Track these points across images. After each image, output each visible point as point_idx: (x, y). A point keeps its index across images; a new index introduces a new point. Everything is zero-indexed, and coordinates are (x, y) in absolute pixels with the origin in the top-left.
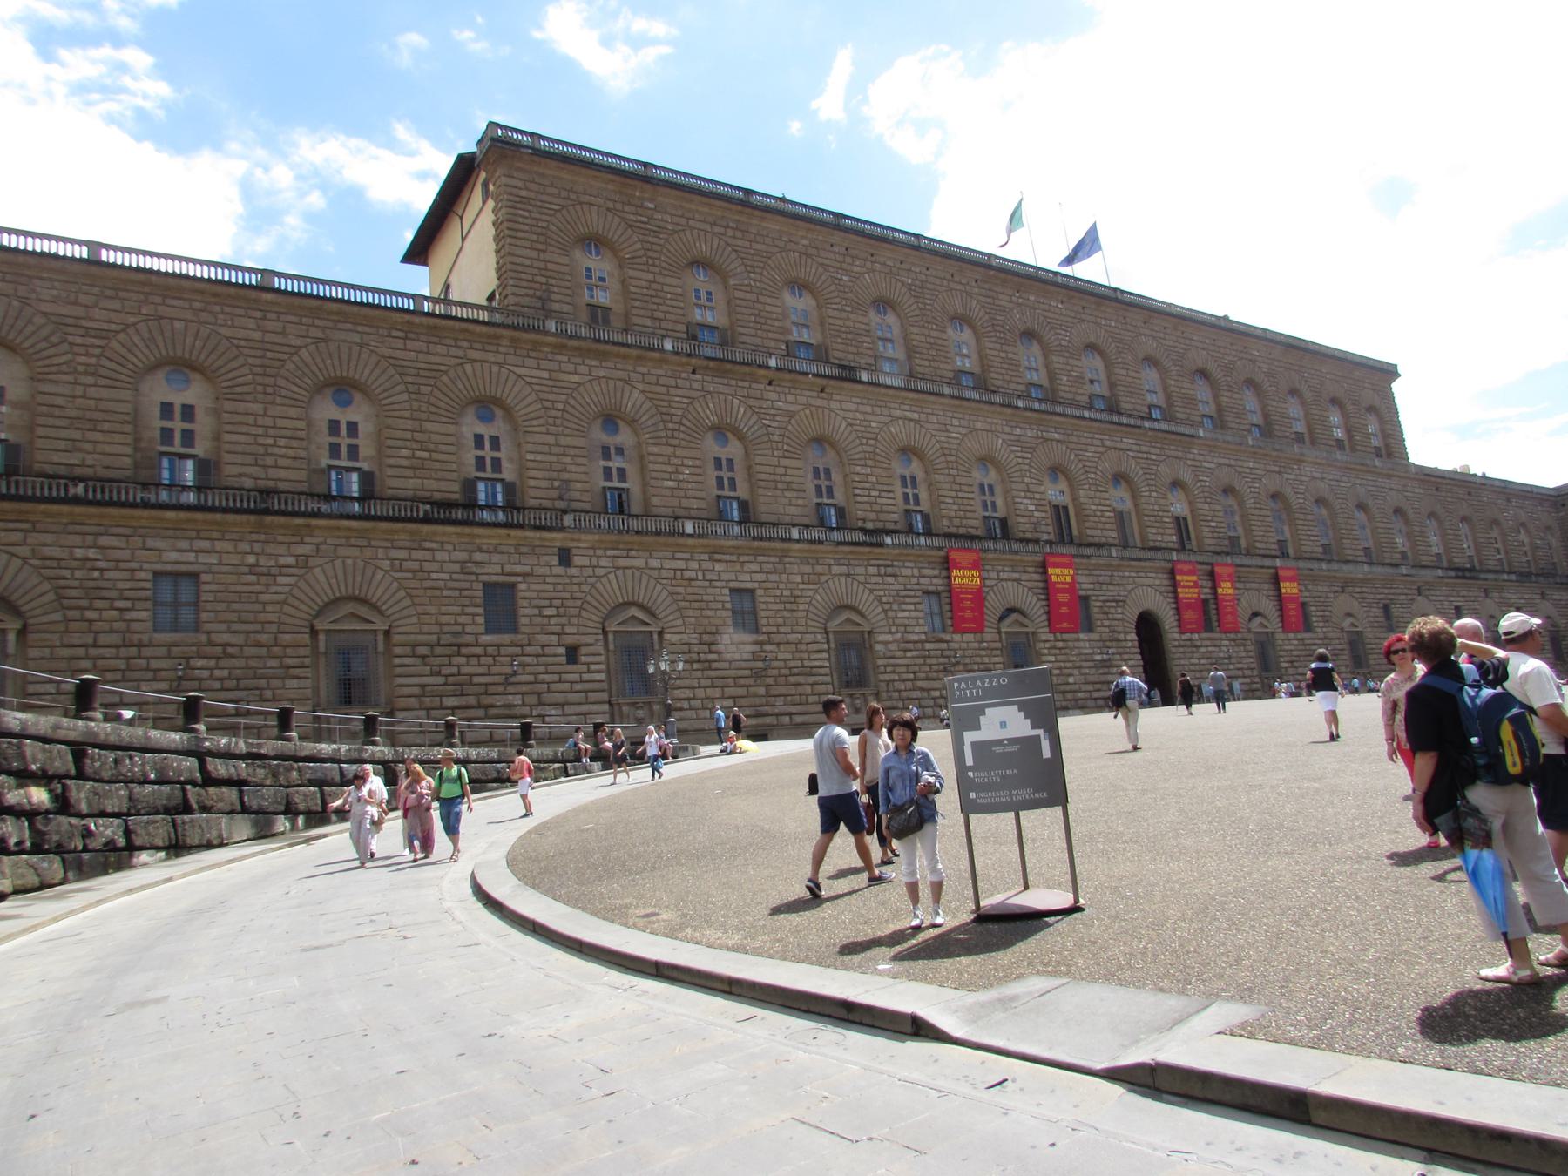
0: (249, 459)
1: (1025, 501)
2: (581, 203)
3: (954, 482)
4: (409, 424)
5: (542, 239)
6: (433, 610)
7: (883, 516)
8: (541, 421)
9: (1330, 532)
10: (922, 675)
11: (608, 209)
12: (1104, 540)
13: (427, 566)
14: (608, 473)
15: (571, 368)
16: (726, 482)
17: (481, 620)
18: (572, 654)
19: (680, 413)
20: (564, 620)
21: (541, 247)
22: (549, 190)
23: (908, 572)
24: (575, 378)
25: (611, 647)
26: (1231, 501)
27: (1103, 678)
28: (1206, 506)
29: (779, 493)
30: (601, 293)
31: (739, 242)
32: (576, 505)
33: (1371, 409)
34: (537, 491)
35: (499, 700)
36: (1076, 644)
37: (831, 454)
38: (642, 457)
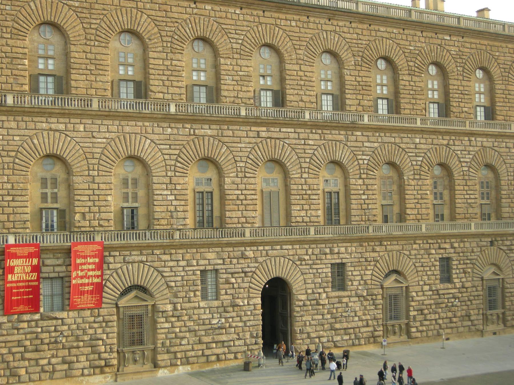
1: (165, 192)
28: (360, 182)
36: (196, 312)
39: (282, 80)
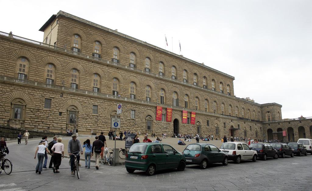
0: (4, 70)
2: (75, 27)
3: (141, 89)
4: (35, 67)
5: (67, 34)
6: (35, 102)
7: (125, 94)
8: (61, 69)
9: (216, 108)
10: (129, 126)
11: (81, 29)
12: (170, 104)
13: (35, 94)
14: (72, 80)
15: (68, 59)
16: (95, 84)
17: (44, 105)
18: (61, 113)
19: (88, 70)
20: (60, 107)
21: (66, 35)
22: (70, 24)
23: (129, 106)
24: (69, 61)
25: (68, 113)
26: (197, 99)
27: (165, 131)
29: (106, 88)
30: (77, 45)
31: (106, 38)
32: (65, 85)
33: (228, 85)
34: (58, 82)
35: (45, 121)
36: (161, 123)
37: (117, 81)
38: (79, 78)
39: (177, 74)
